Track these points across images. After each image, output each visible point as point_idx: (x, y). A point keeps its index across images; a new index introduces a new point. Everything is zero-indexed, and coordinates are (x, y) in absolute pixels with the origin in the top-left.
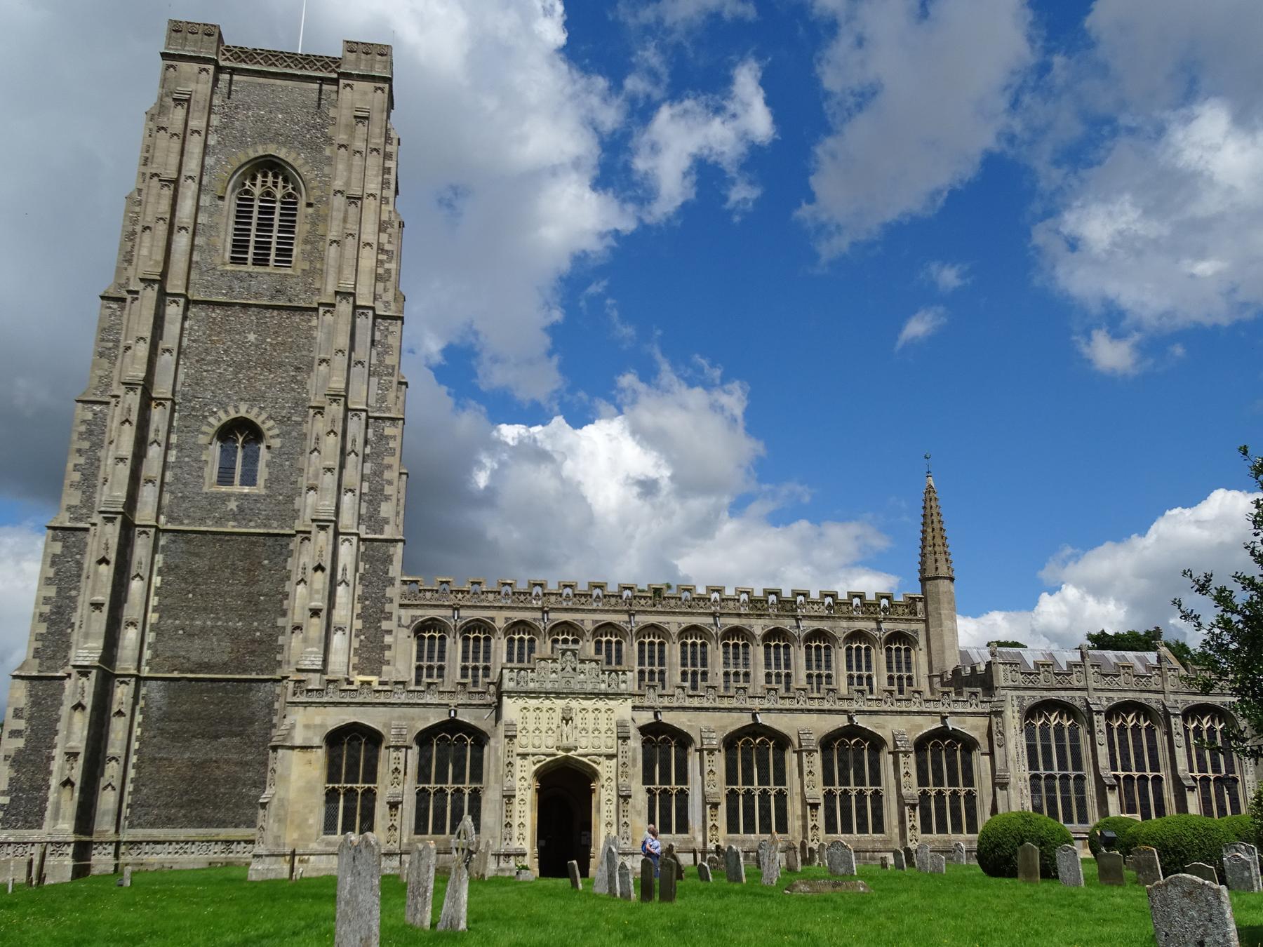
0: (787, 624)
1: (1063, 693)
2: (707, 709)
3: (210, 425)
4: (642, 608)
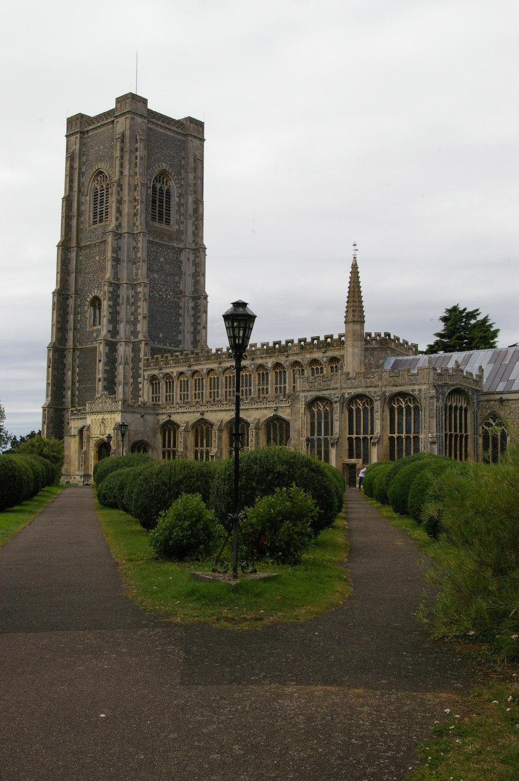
0: (282, 360)
1: (326, 392)
2: (186, 412)
3: (88, 301)
4: (224, 360)
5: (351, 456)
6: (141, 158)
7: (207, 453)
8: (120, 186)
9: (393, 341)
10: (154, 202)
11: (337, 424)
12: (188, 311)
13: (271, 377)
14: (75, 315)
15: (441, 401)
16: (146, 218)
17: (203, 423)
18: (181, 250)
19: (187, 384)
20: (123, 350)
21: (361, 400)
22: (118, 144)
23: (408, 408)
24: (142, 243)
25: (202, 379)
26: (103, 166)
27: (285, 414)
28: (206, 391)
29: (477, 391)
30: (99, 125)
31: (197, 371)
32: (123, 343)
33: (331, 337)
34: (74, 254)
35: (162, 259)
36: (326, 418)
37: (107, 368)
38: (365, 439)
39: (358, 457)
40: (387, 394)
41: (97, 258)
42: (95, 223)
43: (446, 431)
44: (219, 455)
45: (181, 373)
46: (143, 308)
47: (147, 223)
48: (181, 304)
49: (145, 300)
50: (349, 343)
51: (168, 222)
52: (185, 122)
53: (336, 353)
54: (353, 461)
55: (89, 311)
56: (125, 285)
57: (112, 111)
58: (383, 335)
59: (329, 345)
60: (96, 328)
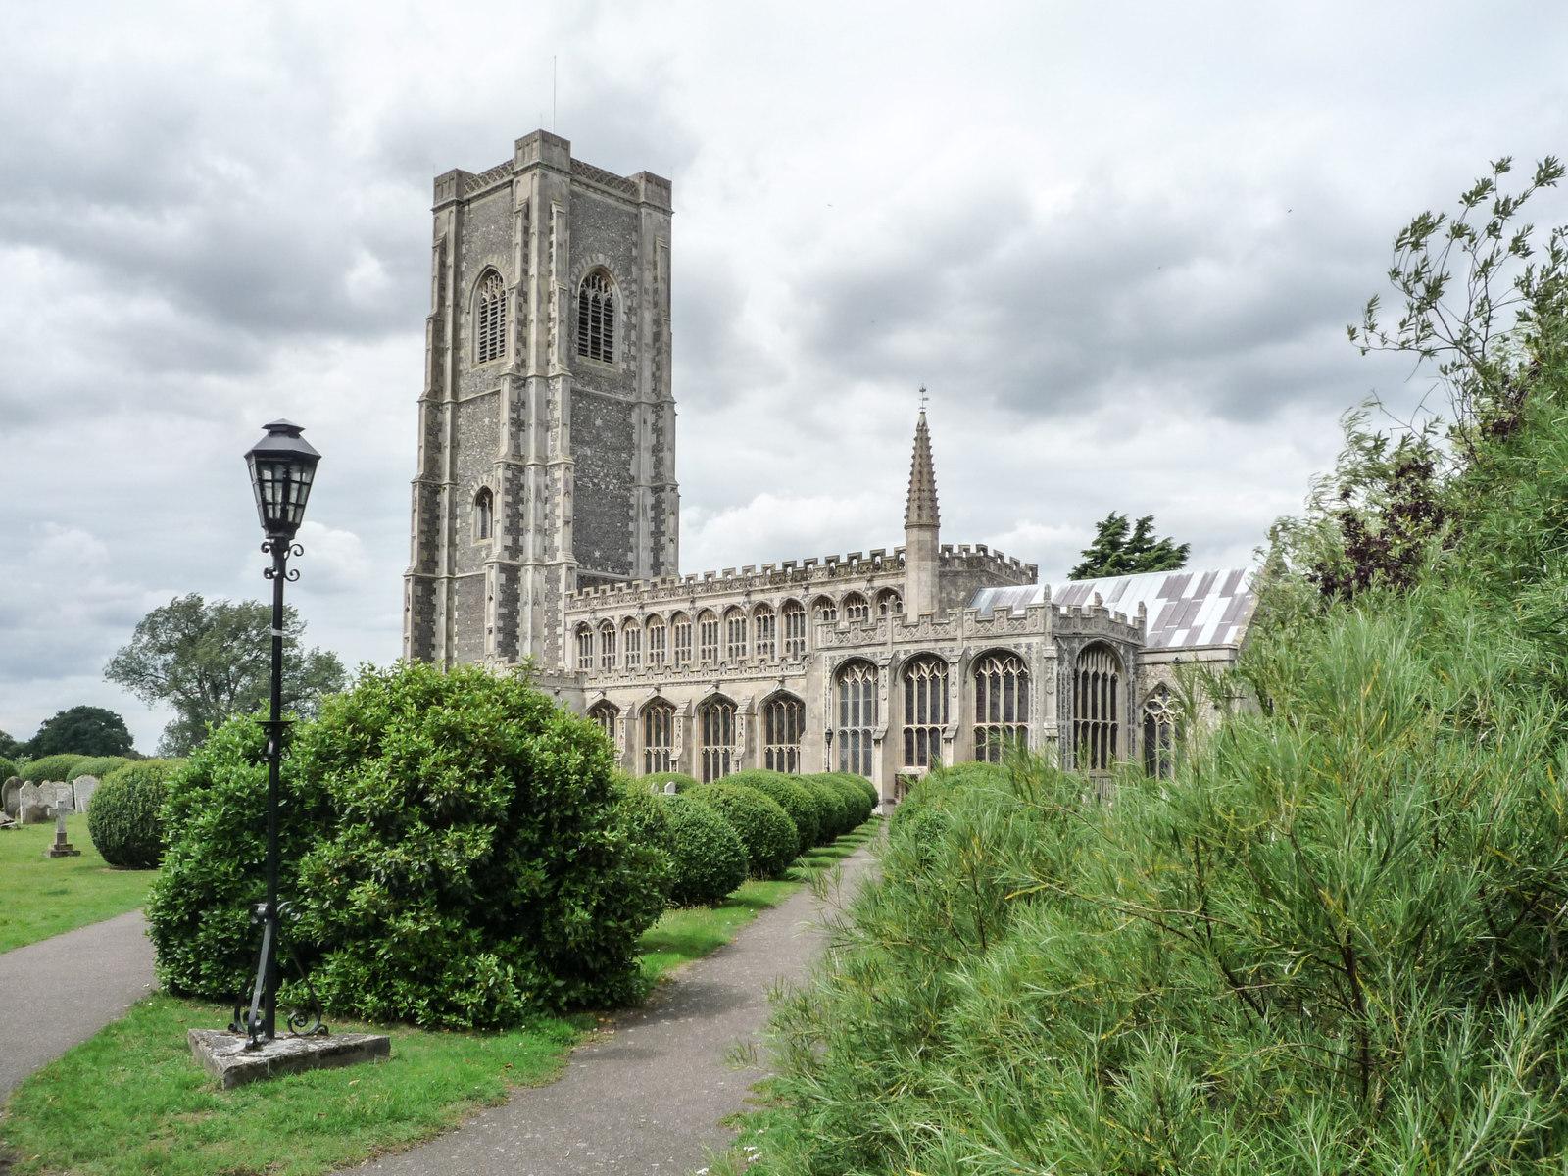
0: (798, 594)
5: (909, 761)
6: (560, 245)
7: (667, 755)
8: (523, 294)
9: (993, 559)
10: (583, 322)
11: (884, 706)
12: (645, 510)
13: (780, 623)
14: (450, 519)
15: (1066, 664)
16: (569, 350)
17: (659, 705)
18: (631, 406)
19: (638, 638)
20: (529, 580)
21: (928, 664)
22: (520, 220)
23: (1008, 676)
24: (558, 393)
25: (663, 628)
26: (494, 261)
27: (794, 688)
28: (670, 649)
29: (1135, 647)
30: (489, 188)
31: (653, 615)
32: (530, 568)
33: (882, 553)
34: (448, 415)
35: (598, 422)
36: (867, 692)
37: (504, 611)
38: (934, 731)
39: (922, 762)
40: (973, 653)
41: (487, 421)
42: (483, 359)
43: (1076, 717)
44: (685, 759)
45: (628, 619)
46: (562, 507)
47: (571, 359)
48: (632, 500)
49: (567, 493)
50: (912, 563)
51: (608, 357)
52: (637, 181)
53: (890, 583)
54: (914, 770)
55: (471, 514)
56: (533, 467)
57: (511, 163)
58: (973, 550)
59: (877, 568)
60: (485, 542)
